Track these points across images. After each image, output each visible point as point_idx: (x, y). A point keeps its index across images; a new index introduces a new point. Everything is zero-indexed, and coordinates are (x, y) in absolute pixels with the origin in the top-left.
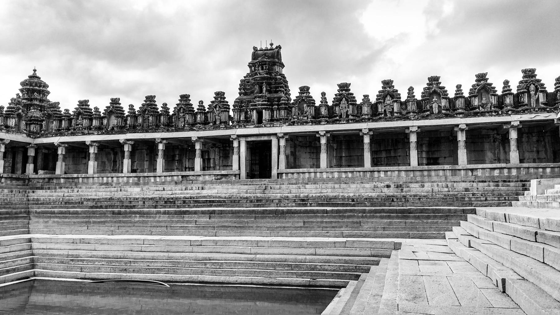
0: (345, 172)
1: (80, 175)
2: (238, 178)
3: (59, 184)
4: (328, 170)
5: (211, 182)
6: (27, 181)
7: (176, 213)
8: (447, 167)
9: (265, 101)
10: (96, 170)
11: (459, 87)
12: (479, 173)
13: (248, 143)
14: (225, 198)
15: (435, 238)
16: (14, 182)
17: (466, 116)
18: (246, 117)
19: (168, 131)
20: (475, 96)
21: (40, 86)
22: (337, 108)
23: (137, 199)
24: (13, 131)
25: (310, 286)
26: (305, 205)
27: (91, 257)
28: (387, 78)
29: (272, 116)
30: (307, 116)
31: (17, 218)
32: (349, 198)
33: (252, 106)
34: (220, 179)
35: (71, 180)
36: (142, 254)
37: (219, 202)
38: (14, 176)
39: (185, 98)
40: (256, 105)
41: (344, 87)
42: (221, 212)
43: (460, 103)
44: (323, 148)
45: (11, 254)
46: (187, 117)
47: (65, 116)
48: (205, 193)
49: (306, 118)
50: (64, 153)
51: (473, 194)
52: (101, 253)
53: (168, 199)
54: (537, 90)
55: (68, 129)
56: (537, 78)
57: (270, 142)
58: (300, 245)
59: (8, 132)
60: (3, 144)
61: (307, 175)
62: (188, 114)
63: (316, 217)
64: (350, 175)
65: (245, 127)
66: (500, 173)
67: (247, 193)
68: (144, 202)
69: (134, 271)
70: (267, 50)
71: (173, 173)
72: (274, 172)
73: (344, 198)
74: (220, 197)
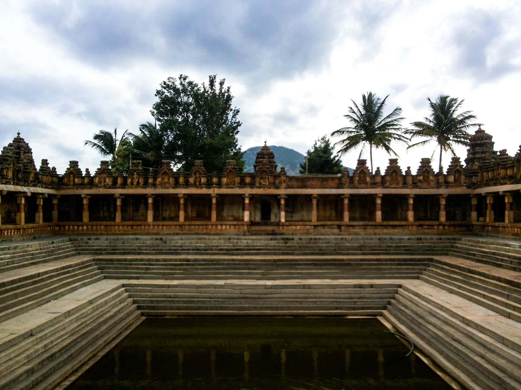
1: (499, 223)
3: (488, 231)
6: (471, 227)
10: (512, 220)
16: (458, 229)
21: (482, 140)
24: (452, 187)
31: (417, 265)
35: (495, 228)
38: (456, 223)
45: (375, 295)
47: (490, 167)
50: (492, 202)
55: (492, 180)
59: (447, 187)
60: (443, 198)
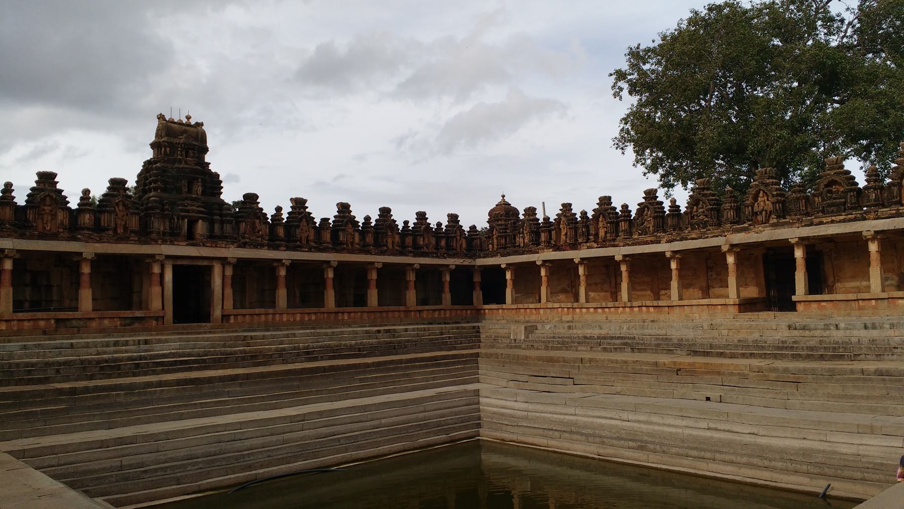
0: (309, 314)
2: (160, 323)
4: (290, 311)
5: (116, 330)
7: (179, 382)
8: (402, 308)
9: (201, 207)
11: (406, 223)
12: (425, 314)
13: (175, 269)
14: (199, 355)
15: (472, 383)
17: (415, 255)
18: (171, 228)
19: (22, 236)
20: (421, 235)
22: (298, 231)
23: (32, 365)
25: (451, 441)
26: (315, 359)
27: (166, 462)
28: (344, 200)
29: (211, 230)
30: (262, 236)
32: (351, 346)
33: (182, 211)
34: (129, 325)
36: (247, 443)
37: (194, 362)
39: (47, 179)
40: (188, 211)
41: (299, 204)
42: (248, 376)
43: (409, 240)
44: (282, 282)
46: (61, 215)
48: (159, 349)
49: (260, 239)
51: (449, 338)
52: (183, 452)
53: (98, 362)
54: (461, 235)
56: (460, 223)
57: (210, 269)
58: (405, 403)
61: (263, 318)
62: (62, 209)
63: (364, 372)
64: (313, 317)
65: (172, 243)
66: (439, 314)
67: (224, 346)
68: (58, 371)
69: (262, 467)
70: (183, 124)
71: (39, 315)
72: (217, 313)
73: (351, 348)
74: (189, 355)
